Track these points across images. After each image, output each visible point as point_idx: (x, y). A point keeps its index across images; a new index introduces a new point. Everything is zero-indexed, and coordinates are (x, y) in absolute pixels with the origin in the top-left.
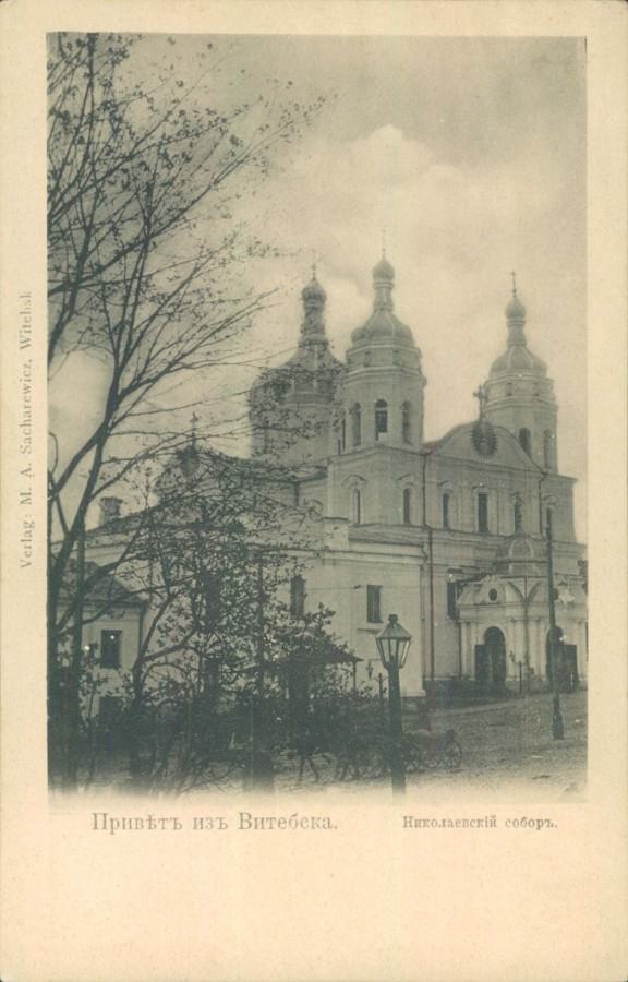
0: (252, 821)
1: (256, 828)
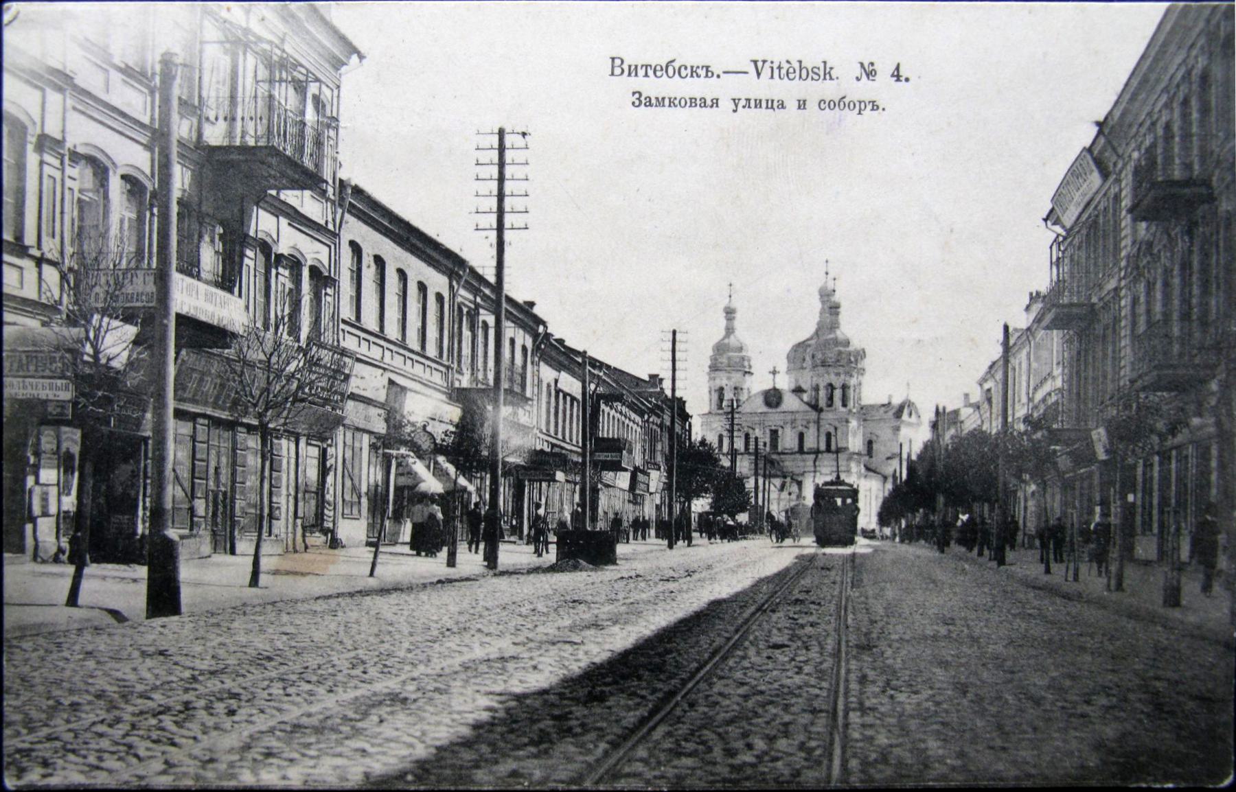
0: (625, 67)
1: (630, 75)
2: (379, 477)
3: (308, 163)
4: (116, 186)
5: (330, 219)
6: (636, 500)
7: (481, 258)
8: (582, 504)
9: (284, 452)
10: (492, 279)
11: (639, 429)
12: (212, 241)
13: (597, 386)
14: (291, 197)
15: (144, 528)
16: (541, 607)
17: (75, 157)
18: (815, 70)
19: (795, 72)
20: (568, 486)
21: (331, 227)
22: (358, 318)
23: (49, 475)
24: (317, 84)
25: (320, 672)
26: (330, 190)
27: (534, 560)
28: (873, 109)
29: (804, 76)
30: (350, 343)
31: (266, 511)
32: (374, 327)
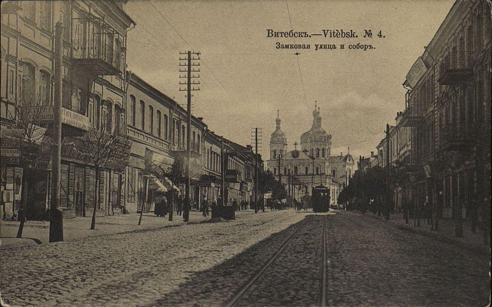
0: (274, 33)
1: (275, 36)
2: (142, 186)
3: (114, 65)
4: (38, 74)
5: (123, 86)
6: (242, 194)
7: (181, 100)
8: (222, 196)
9: (105, 176)
10: (186, 109)
11: (243, 167)
12: (77, 95)
13: (227, 149)
14: (108, 78)
15: (49, 207)
16: (205, 237)
17: (22, 63)
18: (348, 34)
19: (340, 34)
20: (216, 189)
21: (123, 89)
22: (134, 124)
23: (10, 186)
24: (118, 35)
25: (118, 263)
26: (123, 75)
27: (203, 218)
28: (370, 48)
29: (343, 36)
30: (131, 134)
31: (98, 199)
32: (141, 128)
